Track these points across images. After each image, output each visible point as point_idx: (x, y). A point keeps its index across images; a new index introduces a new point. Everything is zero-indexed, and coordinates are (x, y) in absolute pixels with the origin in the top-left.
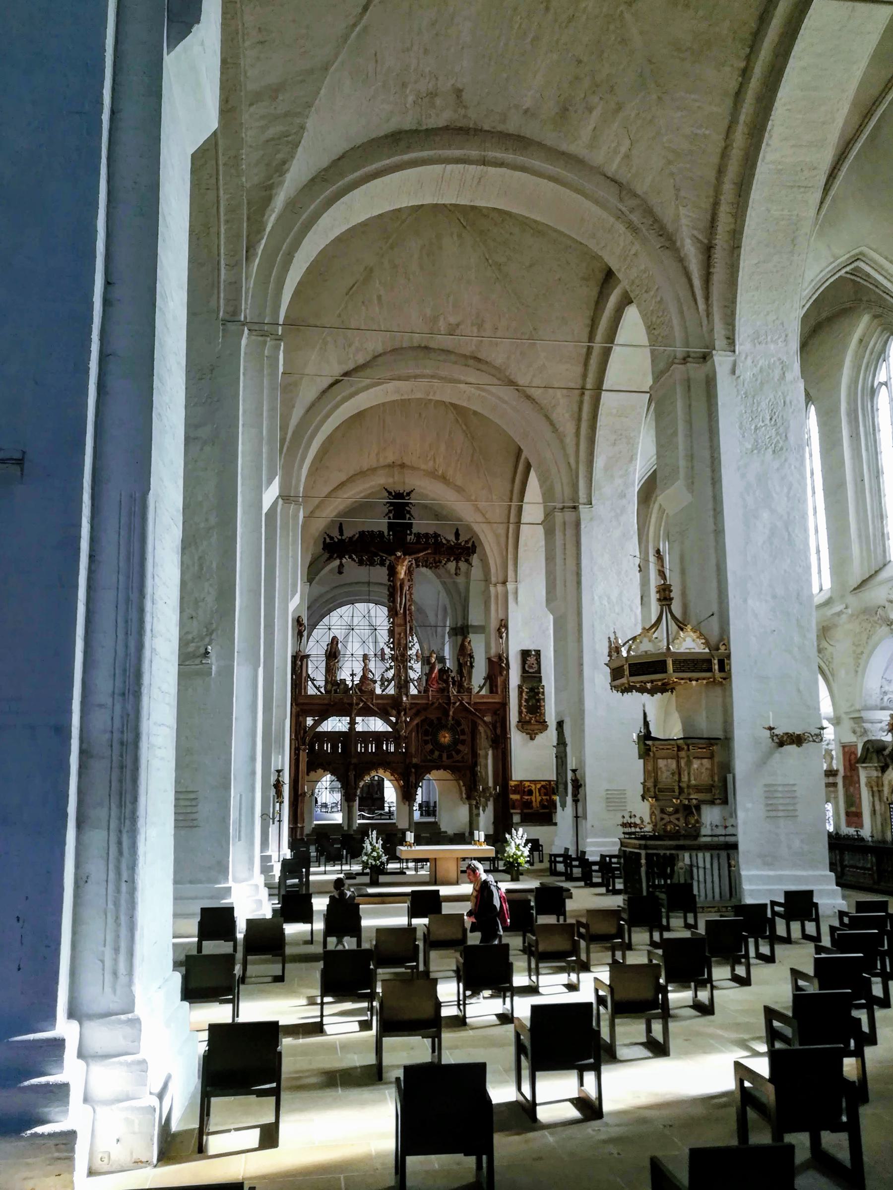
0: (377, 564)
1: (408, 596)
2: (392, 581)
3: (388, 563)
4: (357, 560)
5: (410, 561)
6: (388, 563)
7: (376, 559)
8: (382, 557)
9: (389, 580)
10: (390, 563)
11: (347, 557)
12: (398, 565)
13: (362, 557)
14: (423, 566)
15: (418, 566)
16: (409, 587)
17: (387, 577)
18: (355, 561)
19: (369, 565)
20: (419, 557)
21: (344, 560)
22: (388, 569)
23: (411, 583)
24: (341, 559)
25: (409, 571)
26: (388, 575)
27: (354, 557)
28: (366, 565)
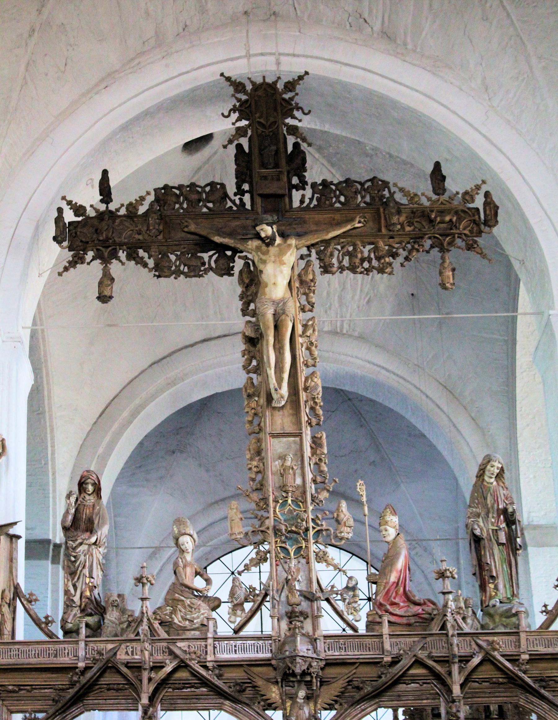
0: (211, 268)
1: (302, 353)
2: (254, 314)
3: (239, 264)
4: (151, 263)
5: (302, 257)
6: (239, 264)
7: (205, 256)
8: (221, 248)
9: (245, 312)
10: (247, 265)
11: (122, 255)
12: (264, 262)
13: (165, 255)
14: (342, 269)
15: (326, 269)
16: (305, 326)
17: (239, 304)
18: (145, 265)
19: (187, 276)
20: (327, 243)
21: (115, 267)
22: (241, 280)
23: (309, 315)
24: (106, 261)
25: (302, 282)
26: (241, 297)
27: (141, 252)
28: (178, 273)
